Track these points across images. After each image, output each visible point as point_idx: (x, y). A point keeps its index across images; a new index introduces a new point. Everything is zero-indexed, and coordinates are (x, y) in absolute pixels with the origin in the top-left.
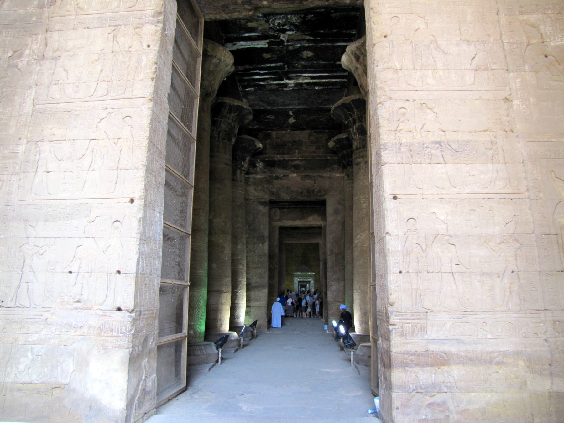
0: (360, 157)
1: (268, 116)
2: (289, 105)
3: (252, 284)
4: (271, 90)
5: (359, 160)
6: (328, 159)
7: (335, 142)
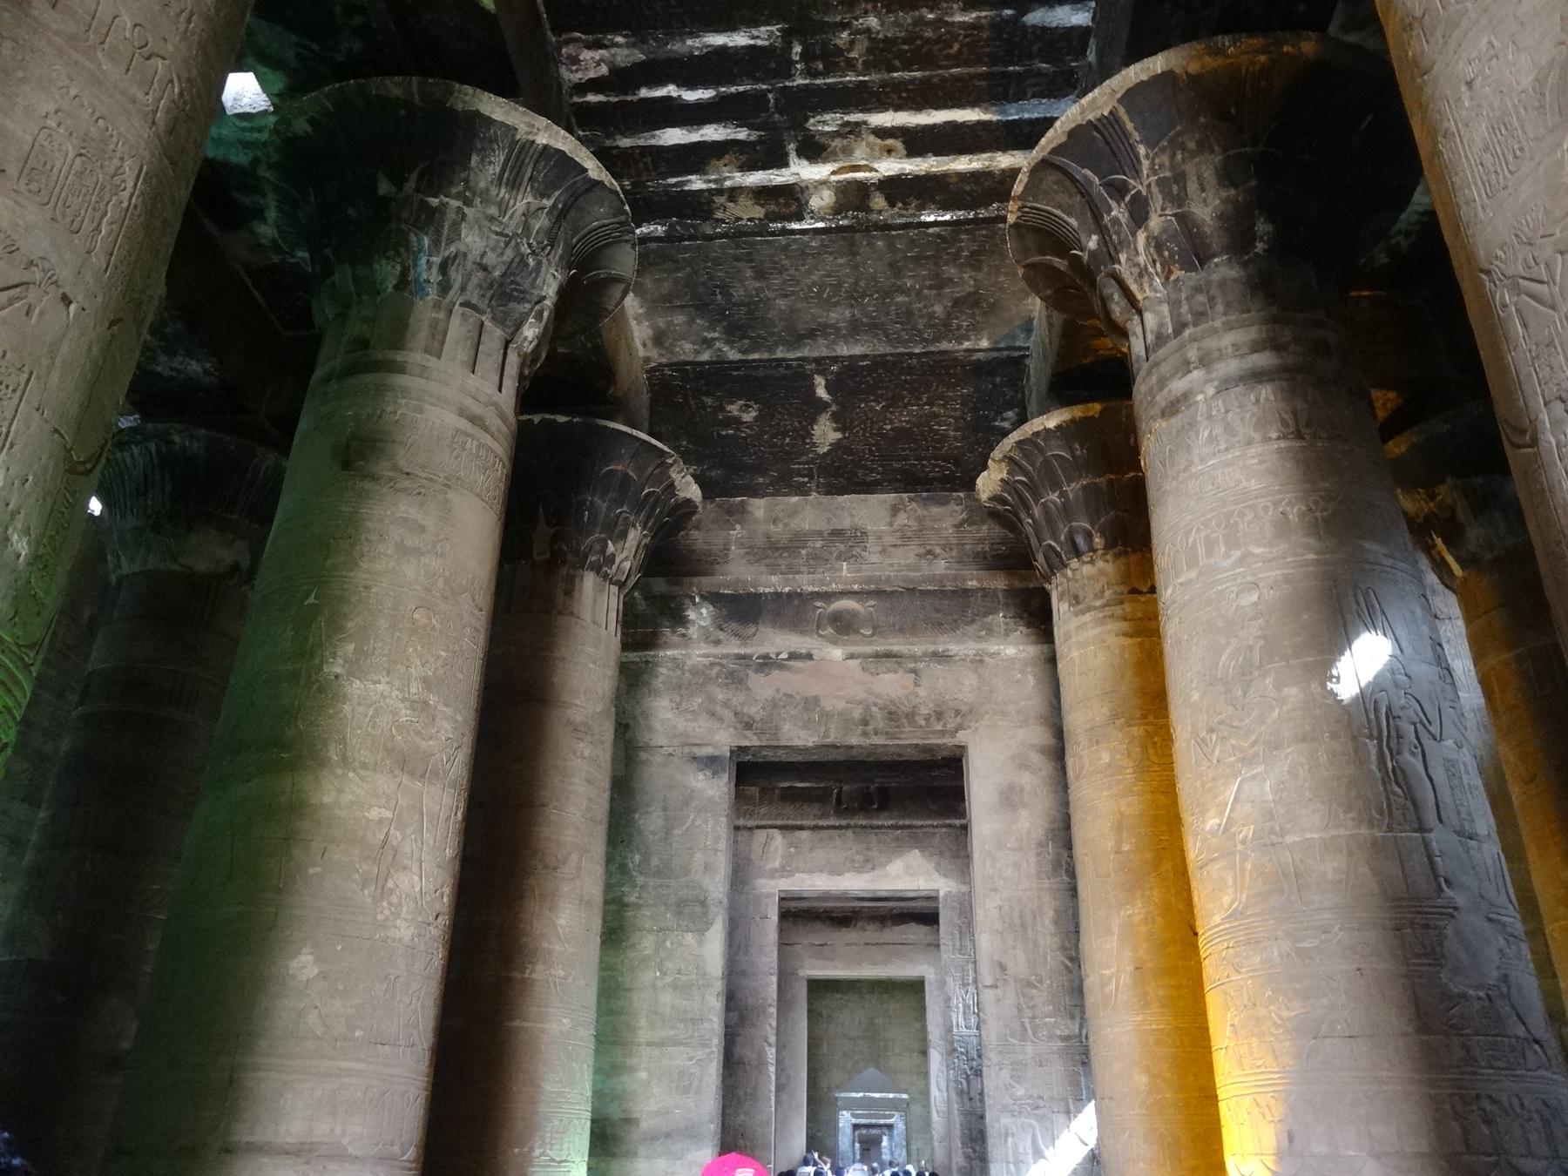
0: (1185, 367)
1: (733, 409)
2: (812, 334)
3: (646, 1124)
4: (738, 234)
5: (1178, 386)
6: (966, 590)
7: (1010, 460)
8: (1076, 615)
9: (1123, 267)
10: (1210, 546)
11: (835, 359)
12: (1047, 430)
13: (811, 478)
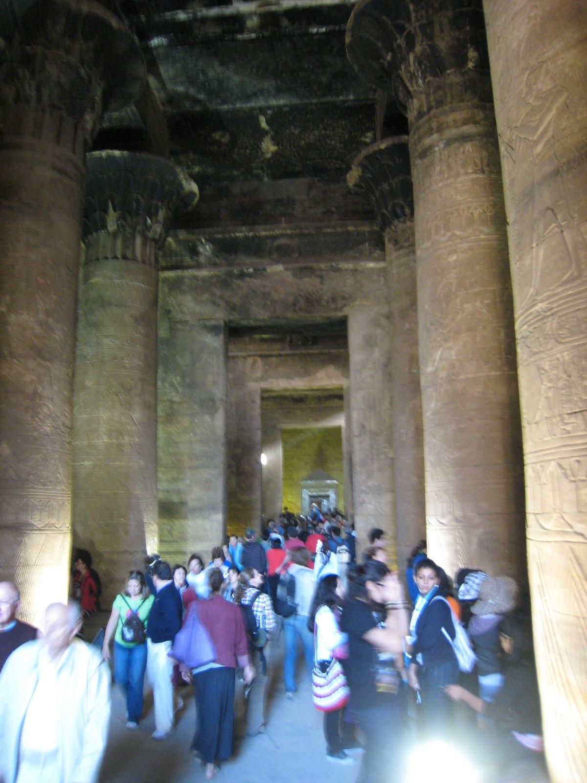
0: (430, 132)
2: (255, 95)
3: (191, 504)
5: (427, 141)
6: (349, 233)
7: (362, 165)
8: (396, 250)
9: (402, 72)
10: (437, 229)
11: (269, 108)
12: (381, 151)
13: (263, 170)
